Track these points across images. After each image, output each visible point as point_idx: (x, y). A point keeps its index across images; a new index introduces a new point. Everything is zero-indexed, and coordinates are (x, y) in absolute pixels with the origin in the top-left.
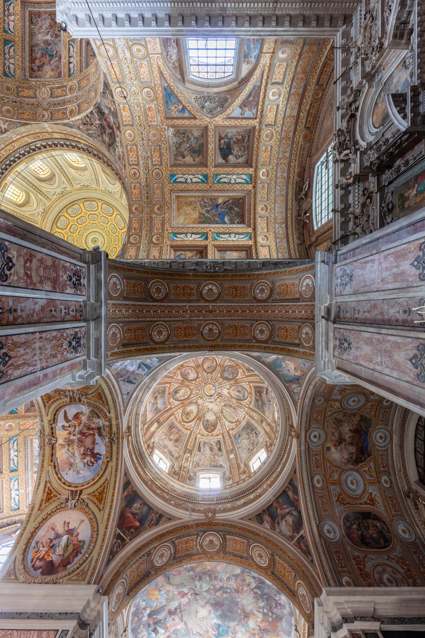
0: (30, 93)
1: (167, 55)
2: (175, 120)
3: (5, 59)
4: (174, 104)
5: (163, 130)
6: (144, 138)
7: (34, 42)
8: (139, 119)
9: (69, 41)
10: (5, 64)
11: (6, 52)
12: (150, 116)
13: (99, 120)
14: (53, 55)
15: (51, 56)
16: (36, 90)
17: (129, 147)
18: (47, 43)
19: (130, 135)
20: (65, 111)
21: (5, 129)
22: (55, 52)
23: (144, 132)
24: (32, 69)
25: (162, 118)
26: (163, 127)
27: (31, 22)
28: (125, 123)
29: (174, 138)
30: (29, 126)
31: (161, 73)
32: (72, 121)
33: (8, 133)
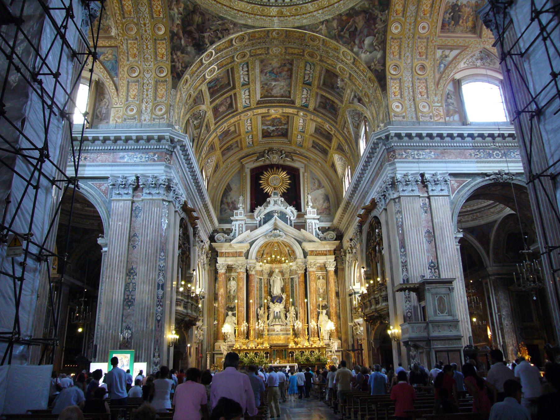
0: (291, 51)
1: (108, 106)
2: (107, 45)
3: (312, 74)
4: (108, 61)
5: (120, 35)
6: (143, 26)
7: (288, 81)
8: (147, 46)
9: (249, 84)
10: (313, 71)
11: (311, 78)
12: (135, 49)
13: (204, 37)
14: (269, 73)
15: (271, 72)
16: (285, 52)
17: (162, 16)
18: (275, 80)
19: (159, 29)
20: (251, 38)
21: (323, 24)
22: (268, 75)
23: (143, 32)
24: (291, 64)
25: (121, 47)
26: (120, 38)
27: (290, 92)
28: (164, 42)
29: (110, 24)
30: (296, 25)
31: (117, 90)
32: (241, 31)
33: (322, 20)
